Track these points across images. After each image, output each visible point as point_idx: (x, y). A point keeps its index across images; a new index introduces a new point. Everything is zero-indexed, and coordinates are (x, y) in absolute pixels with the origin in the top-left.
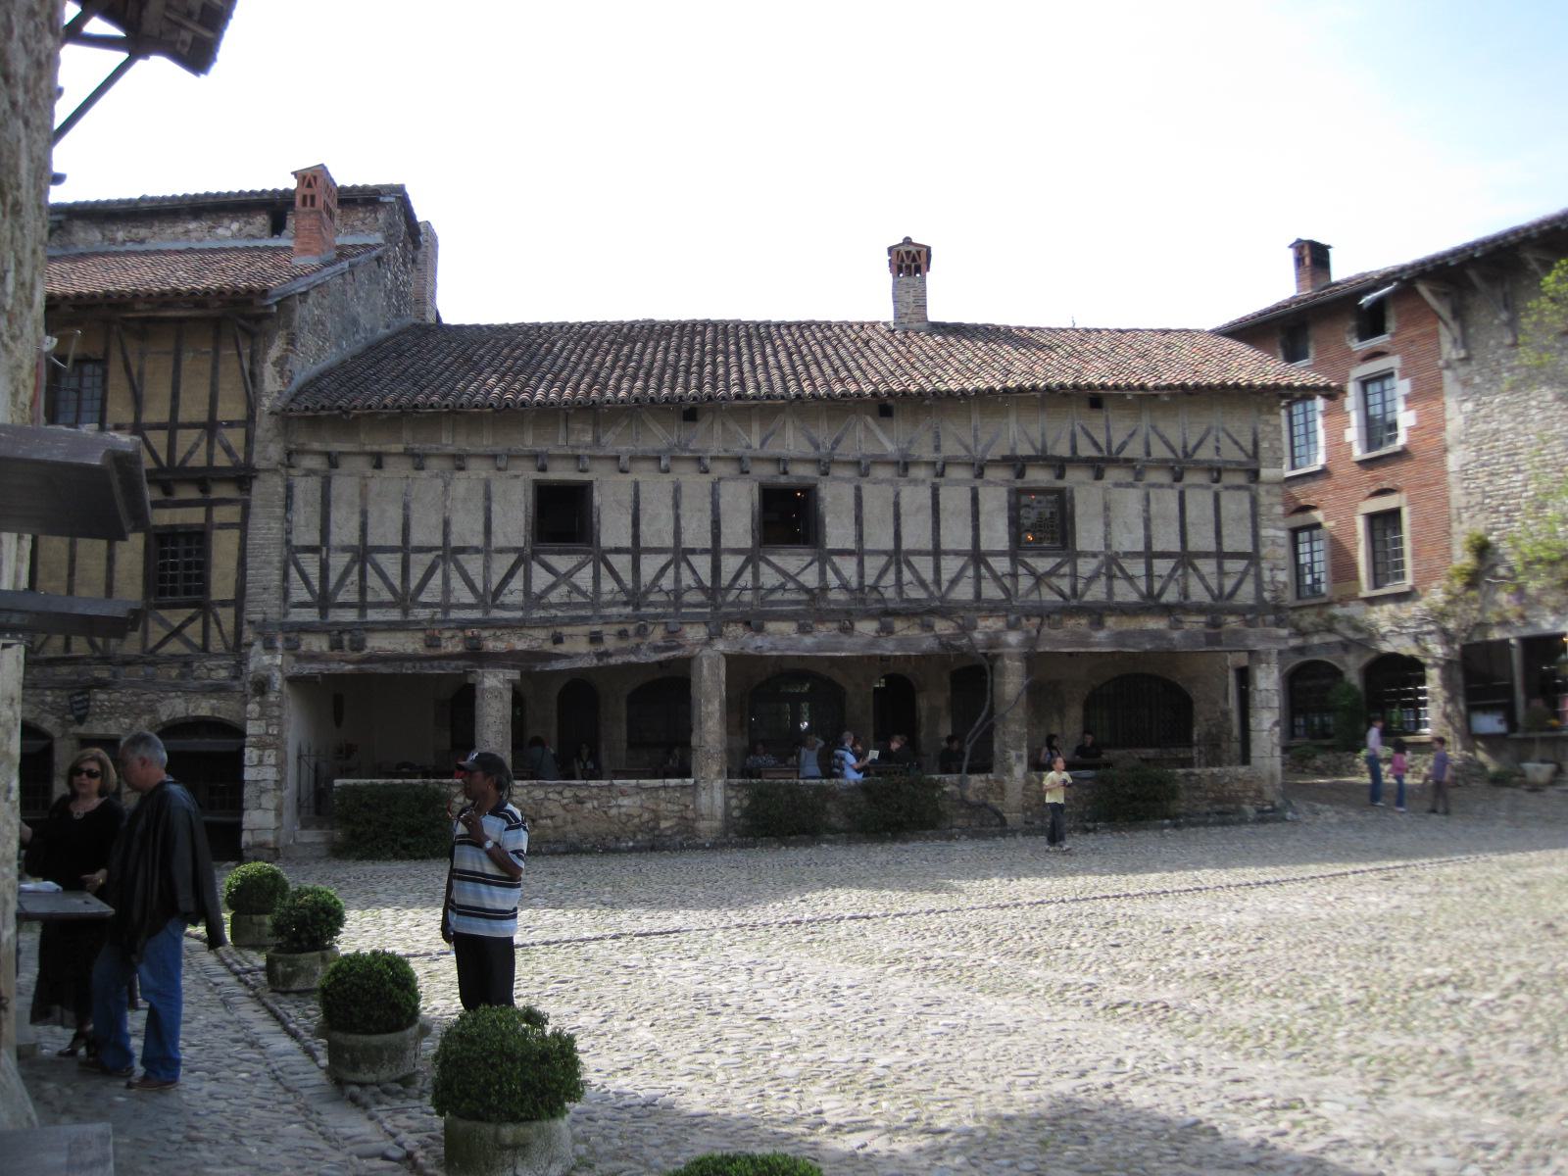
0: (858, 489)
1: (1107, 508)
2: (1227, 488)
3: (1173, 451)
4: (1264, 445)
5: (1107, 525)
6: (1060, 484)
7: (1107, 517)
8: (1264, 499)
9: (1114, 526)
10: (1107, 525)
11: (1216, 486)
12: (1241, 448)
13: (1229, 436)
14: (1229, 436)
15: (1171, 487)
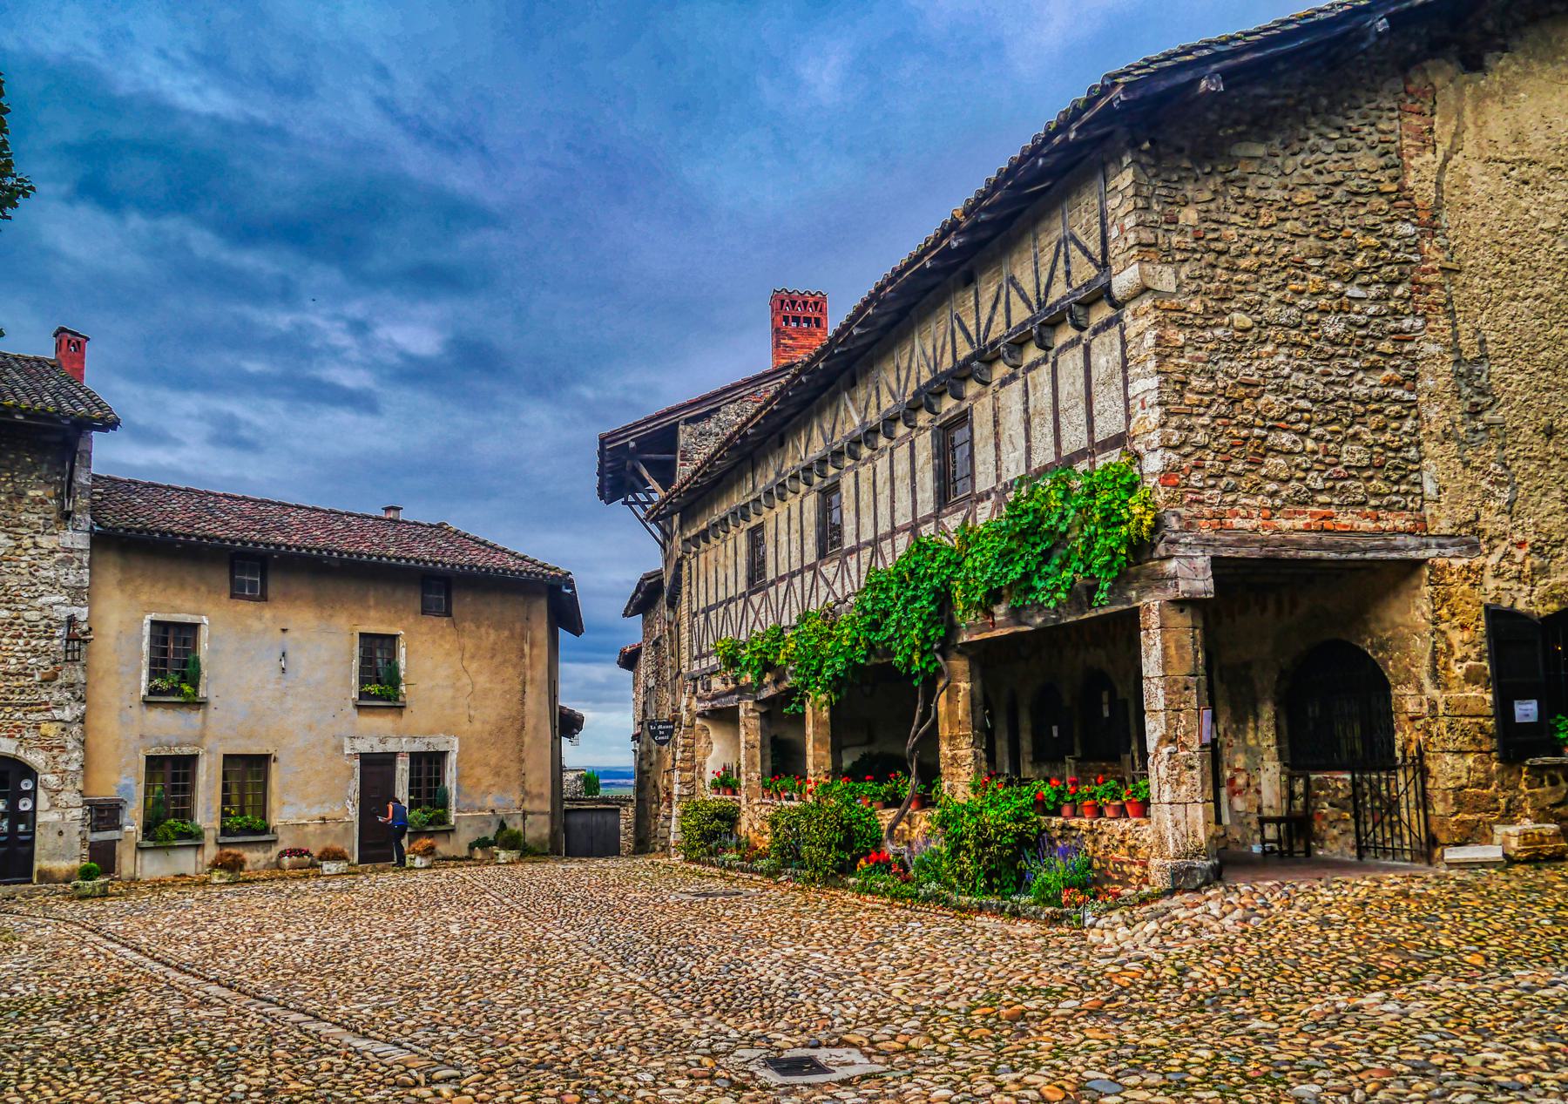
0: (857, 474)
1: (996, 423)
2: (1096, 332)
3: (1030, 306)
4: (1114, 232)
5: (997, 446)
6: (965, 405)
7: (997, 434)
8: (1130, 333)
9: (1003, 447)
10: (997, 446)
11: (1086, 335)
12: (1091, 259)
13: (1078, 244)
14: (1078, 244)
15: (1045, 360)
